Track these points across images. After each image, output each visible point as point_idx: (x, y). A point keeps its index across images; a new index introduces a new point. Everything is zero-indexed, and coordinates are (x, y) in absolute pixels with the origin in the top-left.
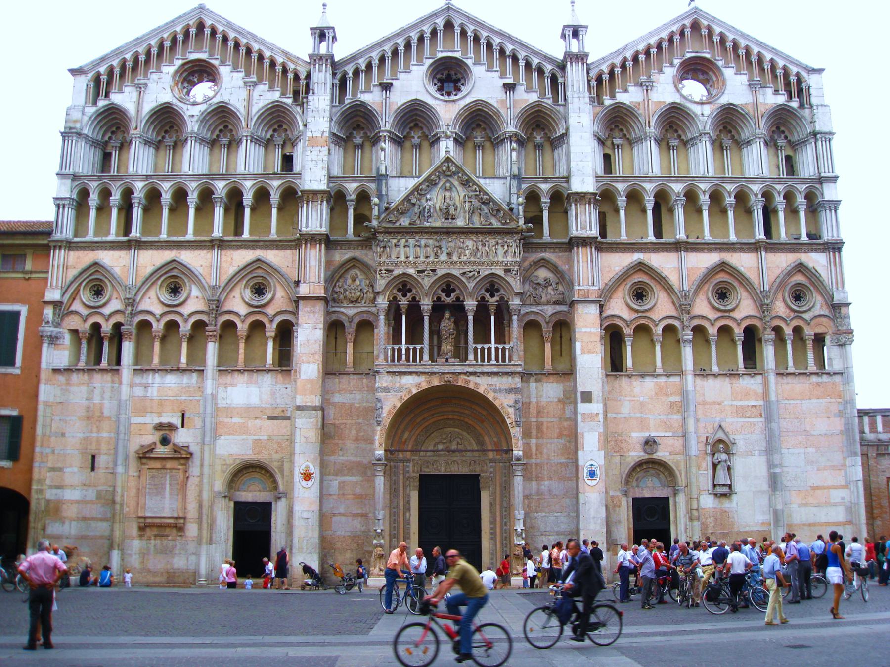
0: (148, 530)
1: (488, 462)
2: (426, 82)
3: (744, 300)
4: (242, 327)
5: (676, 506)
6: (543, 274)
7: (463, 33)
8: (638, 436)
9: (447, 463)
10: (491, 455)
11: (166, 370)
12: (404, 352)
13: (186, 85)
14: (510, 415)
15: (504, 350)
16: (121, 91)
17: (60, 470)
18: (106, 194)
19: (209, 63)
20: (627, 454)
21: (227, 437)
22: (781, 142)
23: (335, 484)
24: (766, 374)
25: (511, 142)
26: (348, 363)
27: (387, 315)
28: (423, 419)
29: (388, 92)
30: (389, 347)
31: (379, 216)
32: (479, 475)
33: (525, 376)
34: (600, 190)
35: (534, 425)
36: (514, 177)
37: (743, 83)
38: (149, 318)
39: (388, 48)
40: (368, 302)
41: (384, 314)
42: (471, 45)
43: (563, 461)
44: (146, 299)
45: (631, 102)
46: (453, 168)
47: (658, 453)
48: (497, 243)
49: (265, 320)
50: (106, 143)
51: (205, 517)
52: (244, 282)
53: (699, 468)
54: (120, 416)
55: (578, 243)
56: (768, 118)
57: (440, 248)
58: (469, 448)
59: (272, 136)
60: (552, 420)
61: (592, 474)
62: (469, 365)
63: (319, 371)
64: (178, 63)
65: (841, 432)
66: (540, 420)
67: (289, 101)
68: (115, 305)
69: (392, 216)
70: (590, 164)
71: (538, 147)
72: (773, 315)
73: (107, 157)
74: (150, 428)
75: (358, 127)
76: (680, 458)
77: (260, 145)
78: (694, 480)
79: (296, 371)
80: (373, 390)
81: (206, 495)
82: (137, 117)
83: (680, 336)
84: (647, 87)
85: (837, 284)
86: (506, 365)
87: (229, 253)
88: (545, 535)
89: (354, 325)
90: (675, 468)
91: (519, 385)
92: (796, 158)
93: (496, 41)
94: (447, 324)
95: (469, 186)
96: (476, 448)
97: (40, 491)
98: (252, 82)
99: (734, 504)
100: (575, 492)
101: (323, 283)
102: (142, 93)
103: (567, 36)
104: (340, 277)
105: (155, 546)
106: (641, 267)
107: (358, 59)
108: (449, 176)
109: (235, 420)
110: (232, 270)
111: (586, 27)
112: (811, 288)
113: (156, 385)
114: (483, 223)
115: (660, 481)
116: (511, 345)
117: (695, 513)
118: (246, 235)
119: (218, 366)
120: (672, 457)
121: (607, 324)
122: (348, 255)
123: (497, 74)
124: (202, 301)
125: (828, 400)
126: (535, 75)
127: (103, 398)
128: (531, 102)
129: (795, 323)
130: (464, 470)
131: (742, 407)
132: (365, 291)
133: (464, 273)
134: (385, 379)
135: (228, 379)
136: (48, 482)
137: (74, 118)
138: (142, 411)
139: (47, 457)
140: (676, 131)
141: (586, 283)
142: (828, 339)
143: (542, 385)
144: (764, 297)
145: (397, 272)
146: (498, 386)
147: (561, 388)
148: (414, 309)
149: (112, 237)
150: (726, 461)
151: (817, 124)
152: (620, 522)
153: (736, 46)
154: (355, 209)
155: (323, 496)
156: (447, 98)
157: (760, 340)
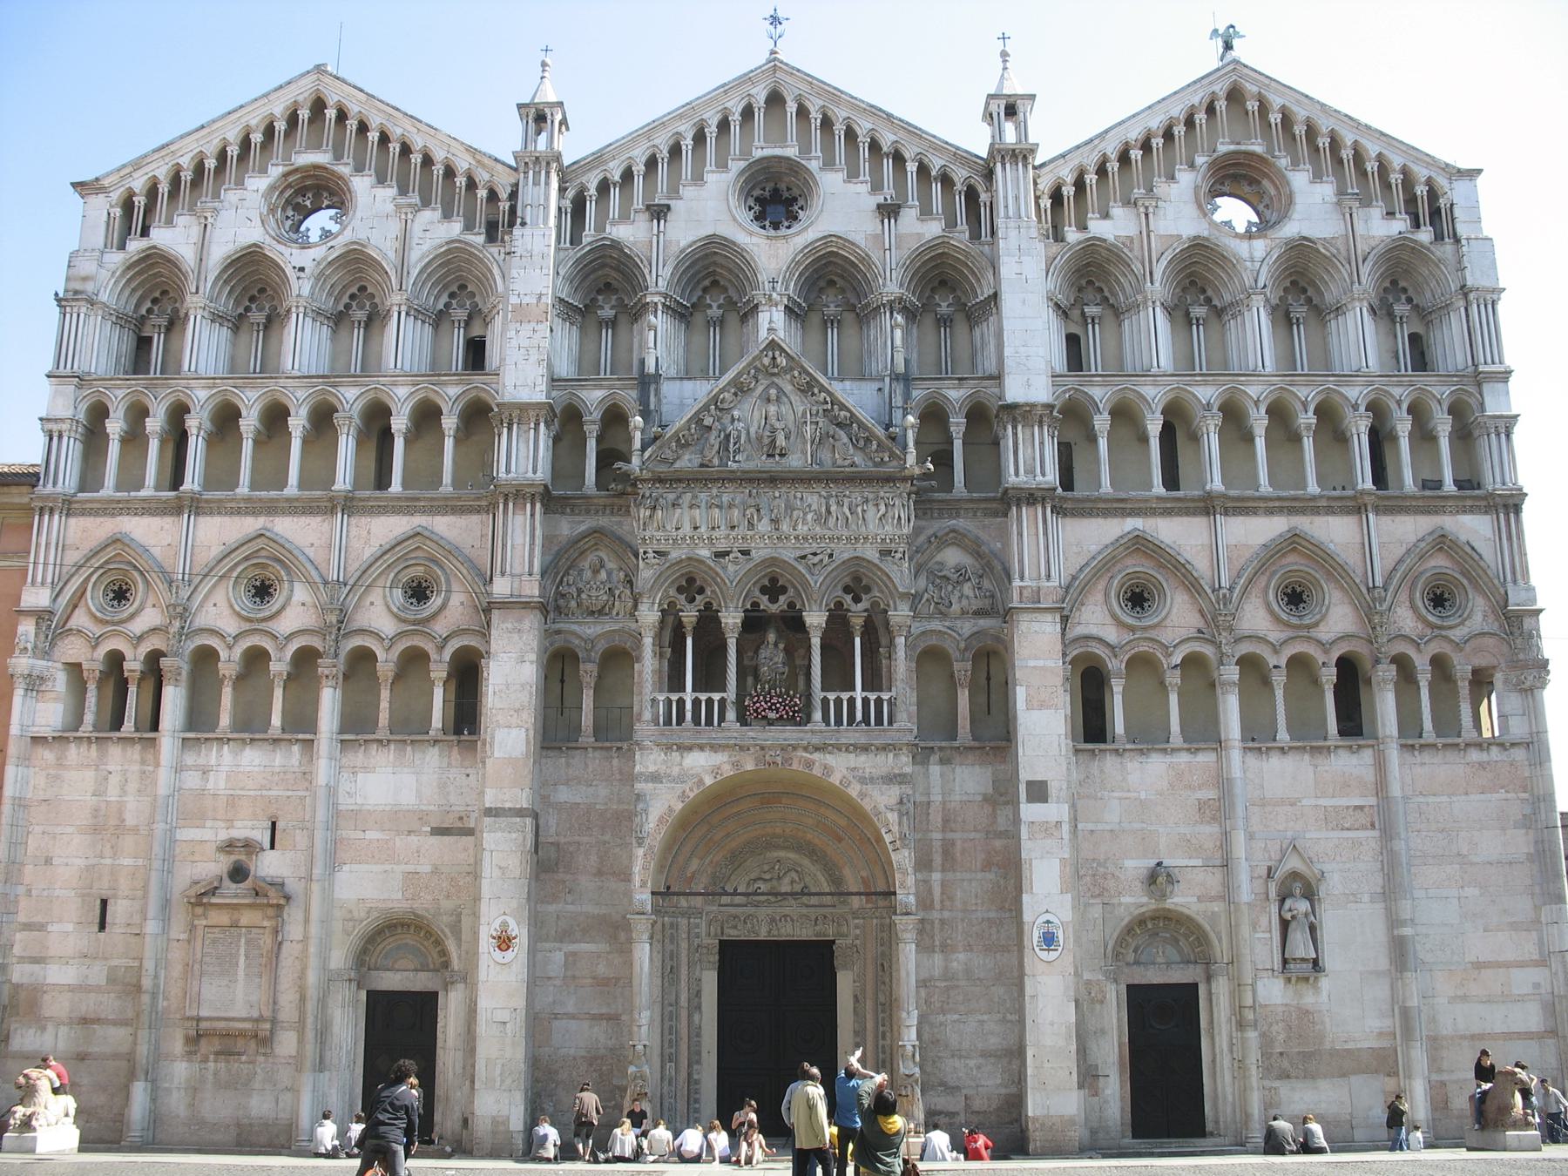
0: (203, 1042)
1: (850, 917)
2: (733, 202)
3: (1335, 605)
4: (386, 662)
5: (1210, 1001)
6: (952, 557)
7: (802, 112)
8: (1136, 865)
9: (773, 920)
10: (856, 902)
11: (243, 740)
12: (689, 706)
13: (290, 213)
14: (891, 825)
15: (879, 702)
16: (169, 222)
17: (41, 927)
18: (138, 413)
19: (333, 173)
20: (1115, 901)
21: (355, 867)
22: (1401, 309)
23: (559, 957)
24: (1381, 747)
25: (891, 313)
26: (583, 728)
27: (658, 636)
28: (728, 835)
29: (662, 222)
30: (661, 697)
31: (643, 449)
32: (833, 942)
33: (921, 755)
34: (1061, 400)
35: (937, 845)
36: (895, 377)
37: (1327, 199)
38: (213, 642)
39: (662, 143)
40: (622, 613)
41: (652, 633)
42: (816, 135)
43: (992, 915)
44: (209, 606)
45: (1116, 237)
46: (782, 361)
47: (1176, 900)
48: (866, 501)
49: (429, 647)
50: (142, 320)
51: (310, 1020)
52: (392, 575)
53: (1254, 926)
54: (155, 826)
55: (1019, 499)
56: (1373, 266)
57: (758, 510)
58: (813, 890)
59: (447, 305)
60: (972, 835)
61: (1049, 940)
62: (812, 731)
63: (528, 742)
64: (276, 171)
65: (1530, 858)
66: (950, 835)
67: (481, 239)
68: (150, 618)
69: (668, 451)
70: (1041, 351)
71: (944, 322)
72: (1393, 633)
73: (143, 344)
74: (211, 849)
75: (608, 288)
76: (1217, 907)
77: (423, 322)
78: (1246, 951)
79: (484, 744)
80: (629, 778)
81: (312, 978)
82: (199, 272)
83: (1216, 675)
84: (1147, 208)
85: (1514, 573)
86: (884, 730)
87: (364, 520)
88: (960, 1057)
89: (596, 655)
90: (1207, 927)
91: (908, 770)
92: (1428, 337)
93: (863, 127)
94: (772, 656)
95: (813, 394)
96: (827, 890)
98: (410, 205)
99: (1325, 994)
100: (1016, 974)
101: (538, 577)
102: (209, 227)
103: (995, 116)
104: (569, 568)
105: (215, 1074)
106: (1140, 544)
107: (606, 162)
108: (774, 375)
109: (370, 835)
110: (368, 553)
111: (1032, 97)
112: (1465, 582)
113: (222, 768)
114: (839, 462)
115: (1180, 951)
116: (893, 694)
117: (1249, 1015)
118: (396, 486)
119: (341, 732)
120: (1202, 907)
121: (1075, 653)
122: (586, 524)
123: (865, 188)
124: (312, 610)
125: (1502, 794)
126: (937, 189)
127: (124, 792)
128: (928, 237)
129: (1434, 648)
130: (805, 933)
132: (617, 592)
133: (804, 557)
134: (652, 757)
135: (358, 758)
136: (17, 950)
137: (83, 273)
138: (198, 817)
139: (17, 902)
140: (1203, 291)
141: (1035, 575)
142: (1498, 678)
143: (954, 769)
144: (1374, 600)
145: (675, 555)
146: (868, 770)
147: (989, 774)
148: (709, 622)
149: (147, 492)
150: (1306, 915)
151: (1468, 273)
152: (1103, 1032)
153: (1311, 132)
154: (599, 440)
155: (535, 981)
156: (772, 233)
157: (1369, 682)
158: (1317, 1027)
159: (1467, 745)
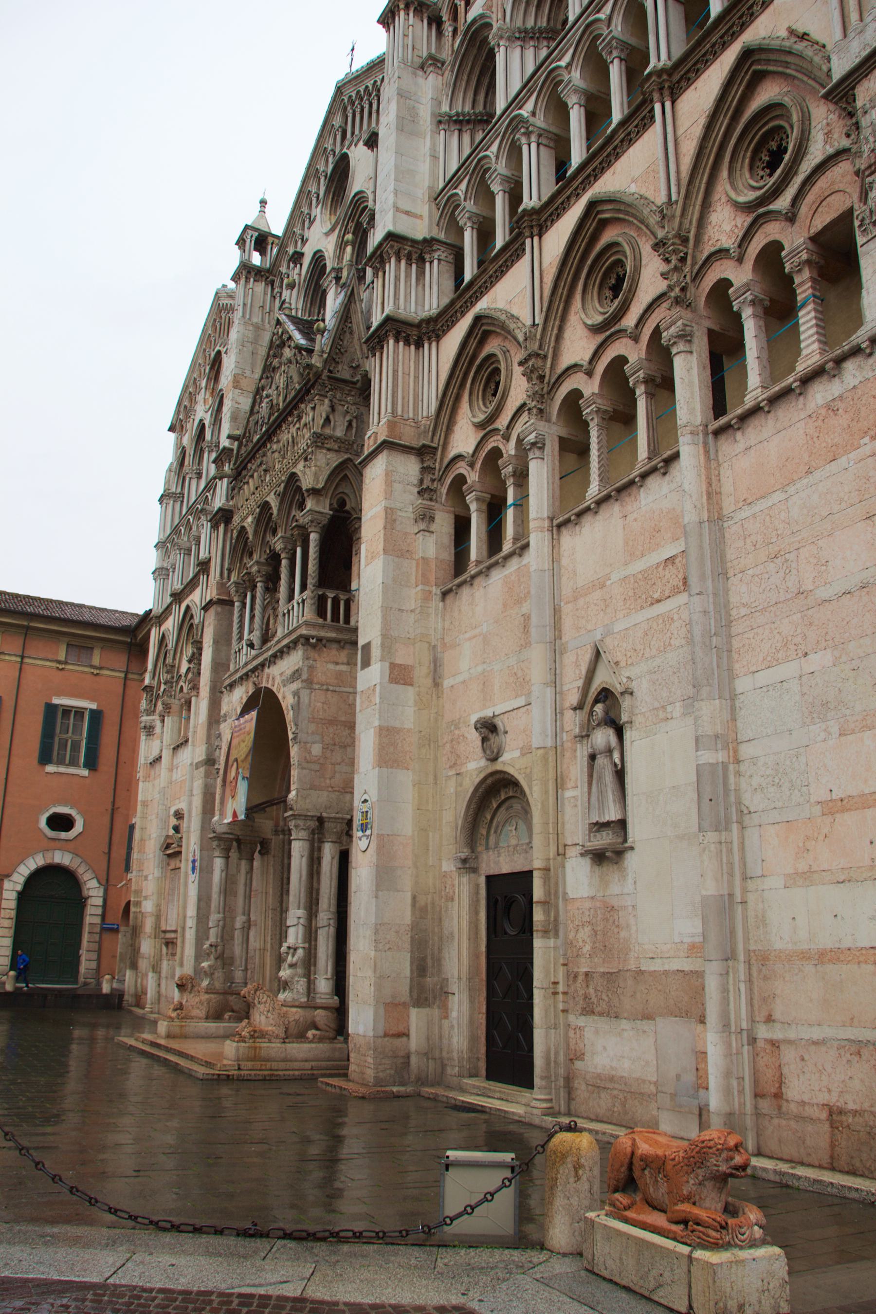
20: (463, 770)
97: (138, 904)
99: (630, 881)
131: (645, 576)
136: (144, 894)
158: (623, 934)
159: (807, 380)
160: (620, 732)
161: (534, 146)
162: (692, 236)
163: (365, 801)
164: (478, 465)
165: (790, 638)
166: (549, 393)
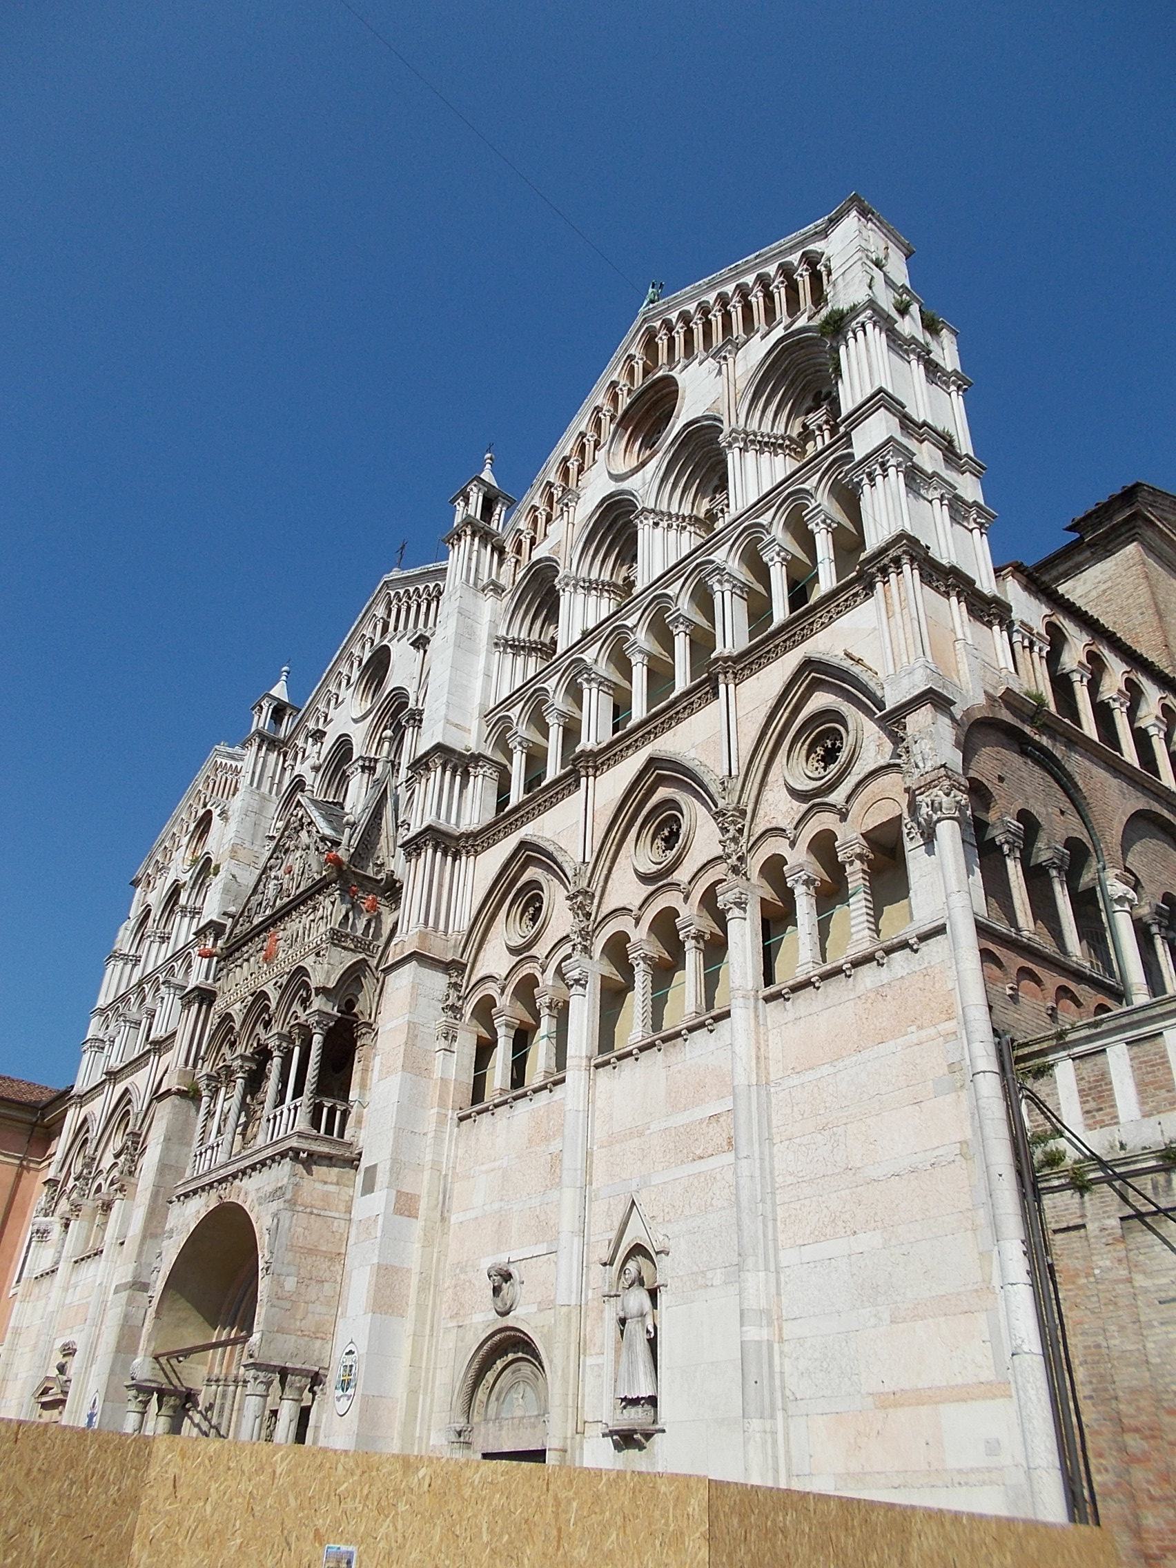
20: (467, 1322)
160: (653, 1294)
161: (594, 691)
162: (749, 810)
163: (351, 1352)
164: (510, 990)
165: (838, 1214)
166: (594, 931)
